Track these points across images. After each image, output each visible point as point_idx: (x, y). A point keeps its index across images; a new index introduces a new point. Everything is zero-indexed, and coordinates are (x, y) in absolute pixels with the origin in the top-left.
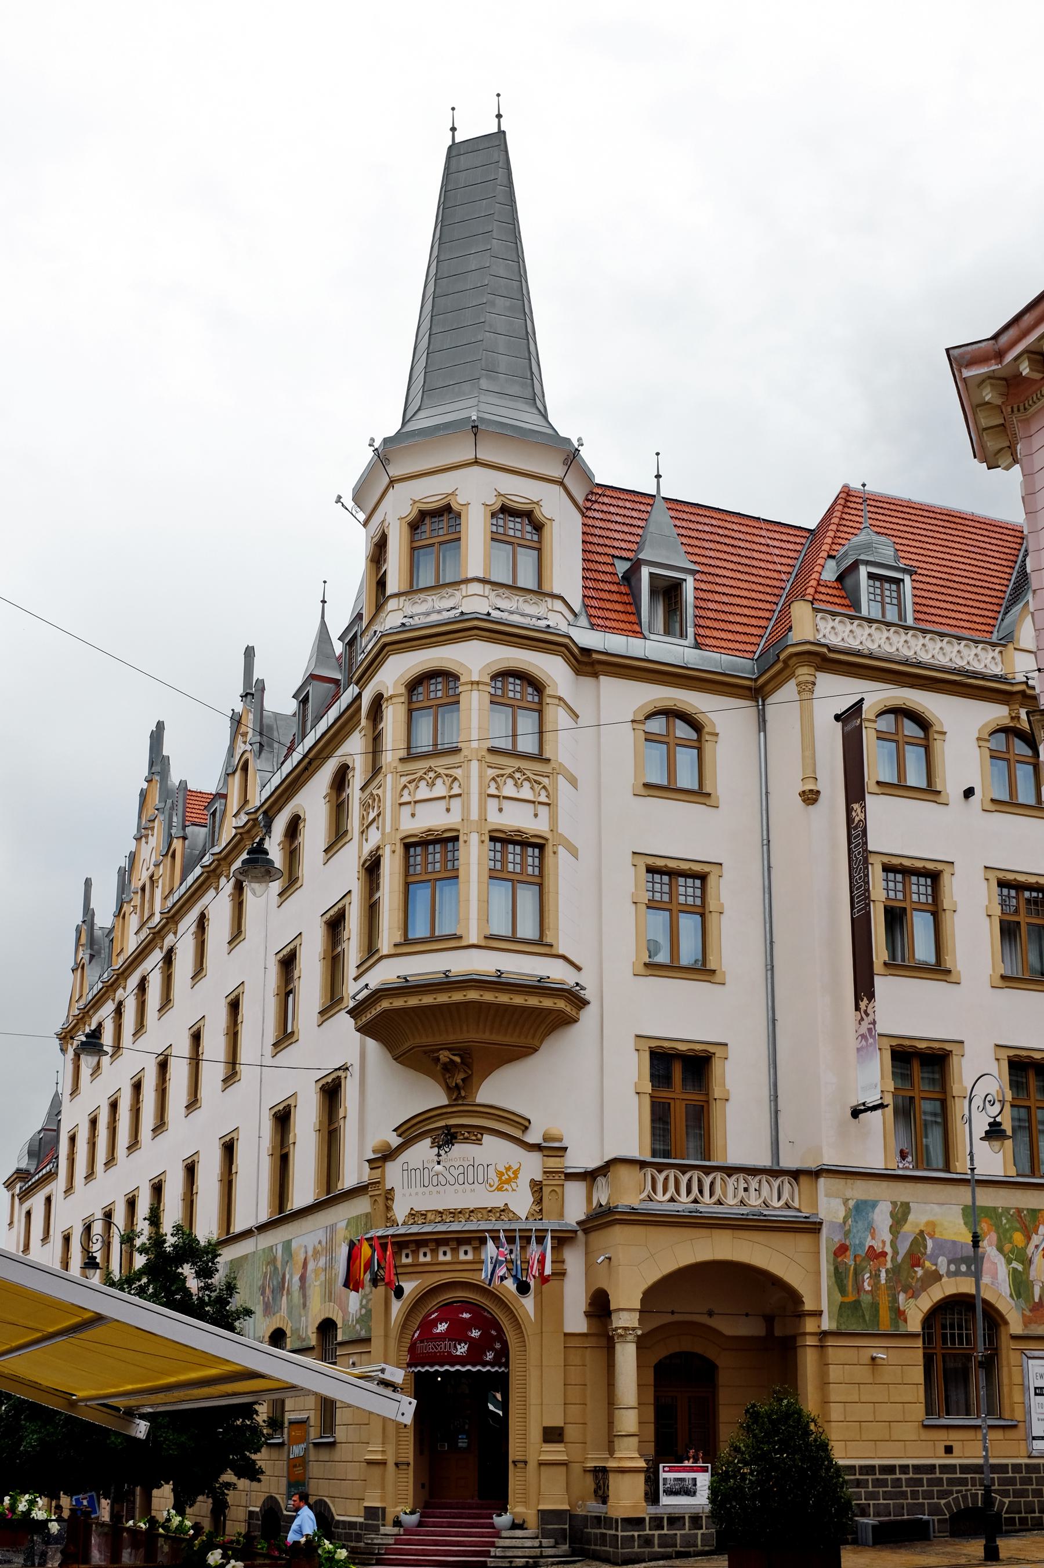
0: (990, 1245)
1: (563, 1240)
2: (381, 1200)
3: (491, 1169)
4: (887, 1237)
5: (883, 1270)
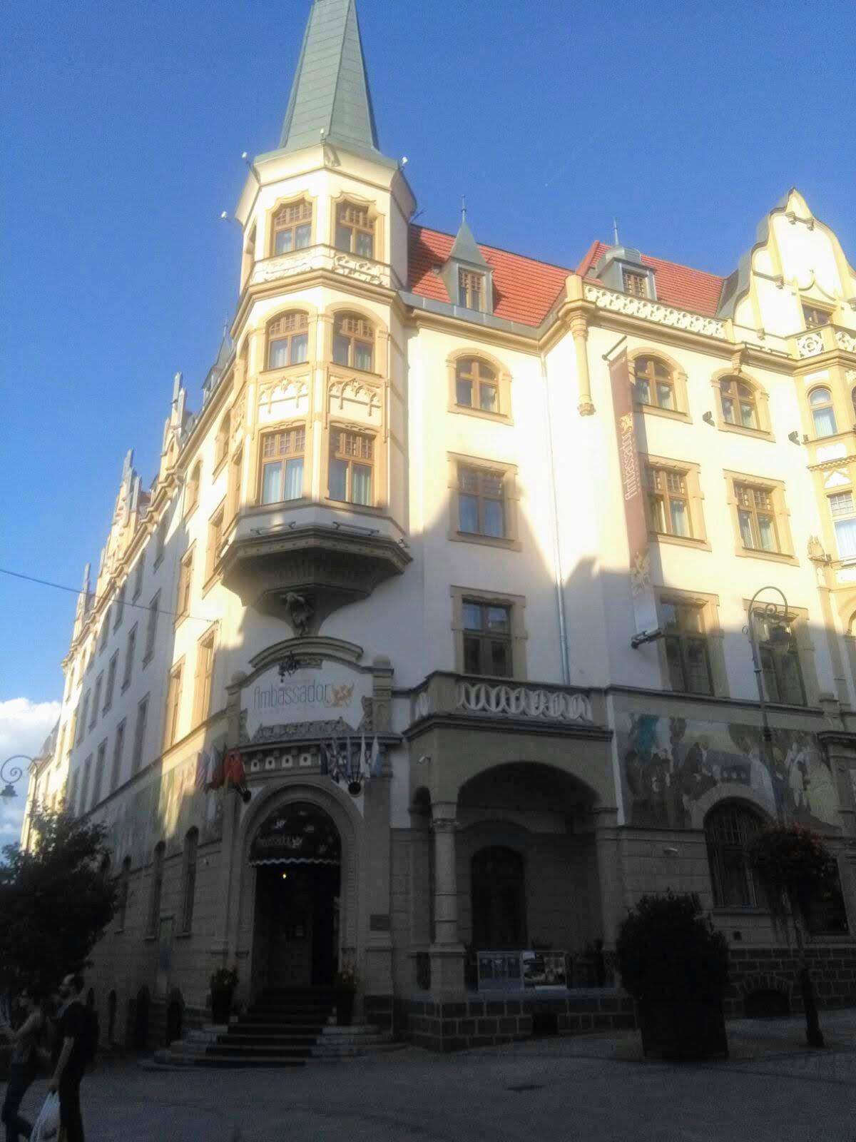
0: (754, 756)
1: (390, 746)
3: (329, 689)
4: (668, 746)
5: (668, 775)
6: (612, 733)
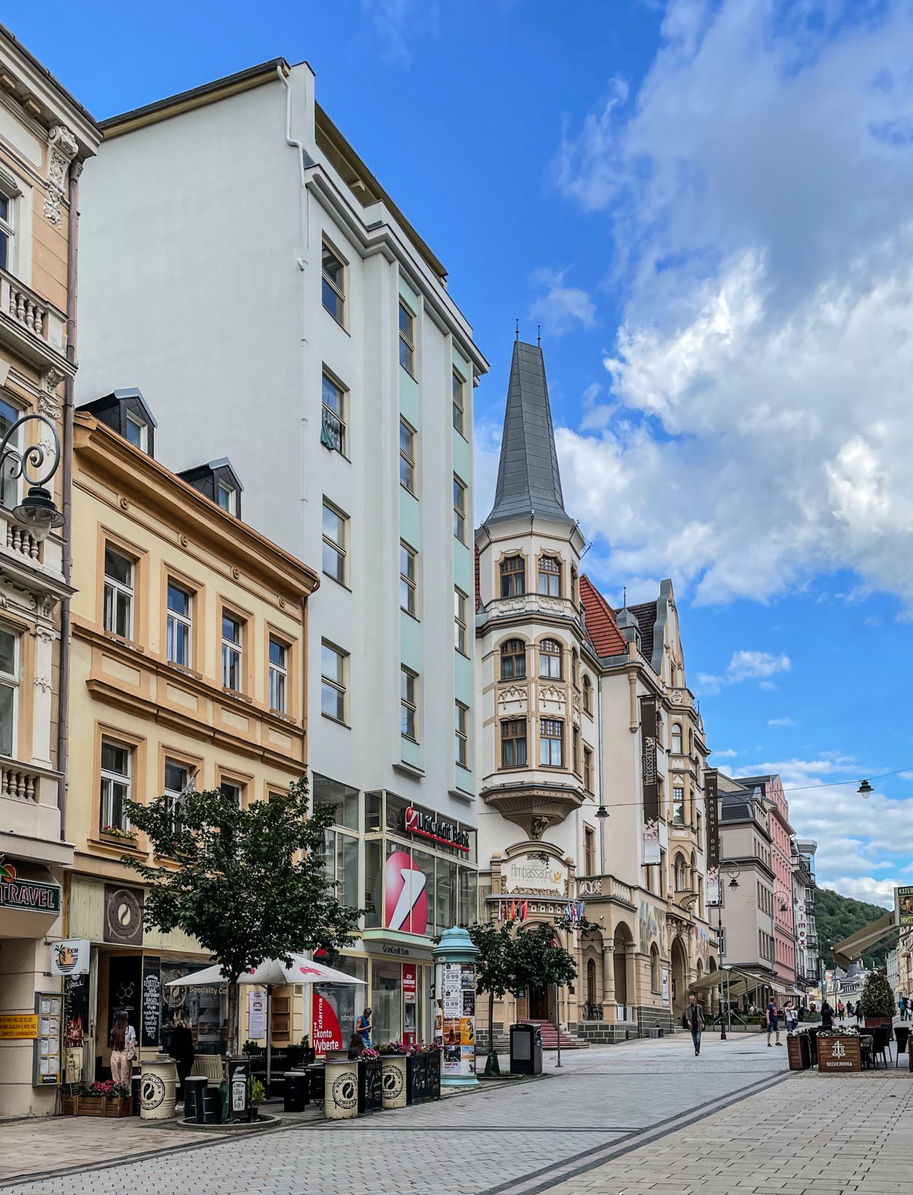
2: (500, 881)
6: (636, 909)
